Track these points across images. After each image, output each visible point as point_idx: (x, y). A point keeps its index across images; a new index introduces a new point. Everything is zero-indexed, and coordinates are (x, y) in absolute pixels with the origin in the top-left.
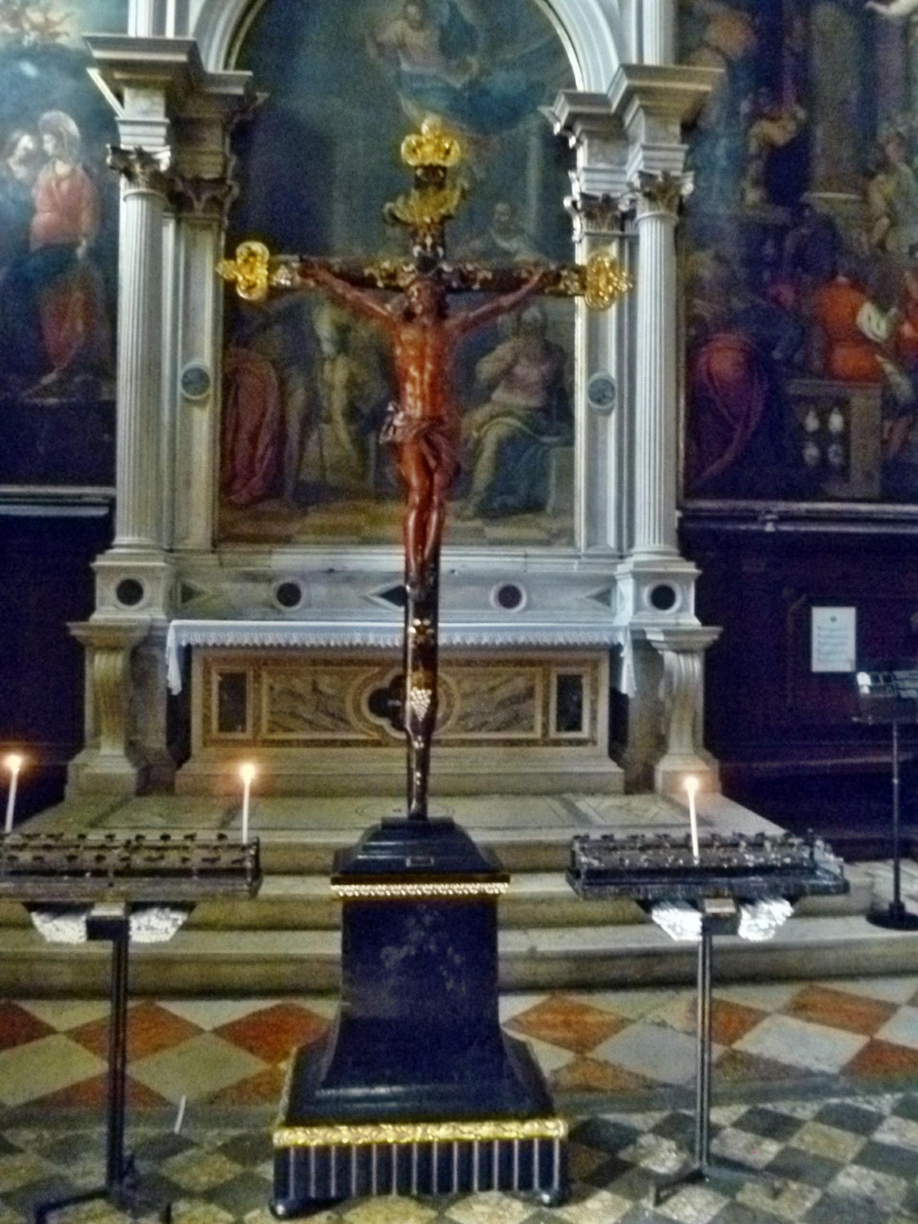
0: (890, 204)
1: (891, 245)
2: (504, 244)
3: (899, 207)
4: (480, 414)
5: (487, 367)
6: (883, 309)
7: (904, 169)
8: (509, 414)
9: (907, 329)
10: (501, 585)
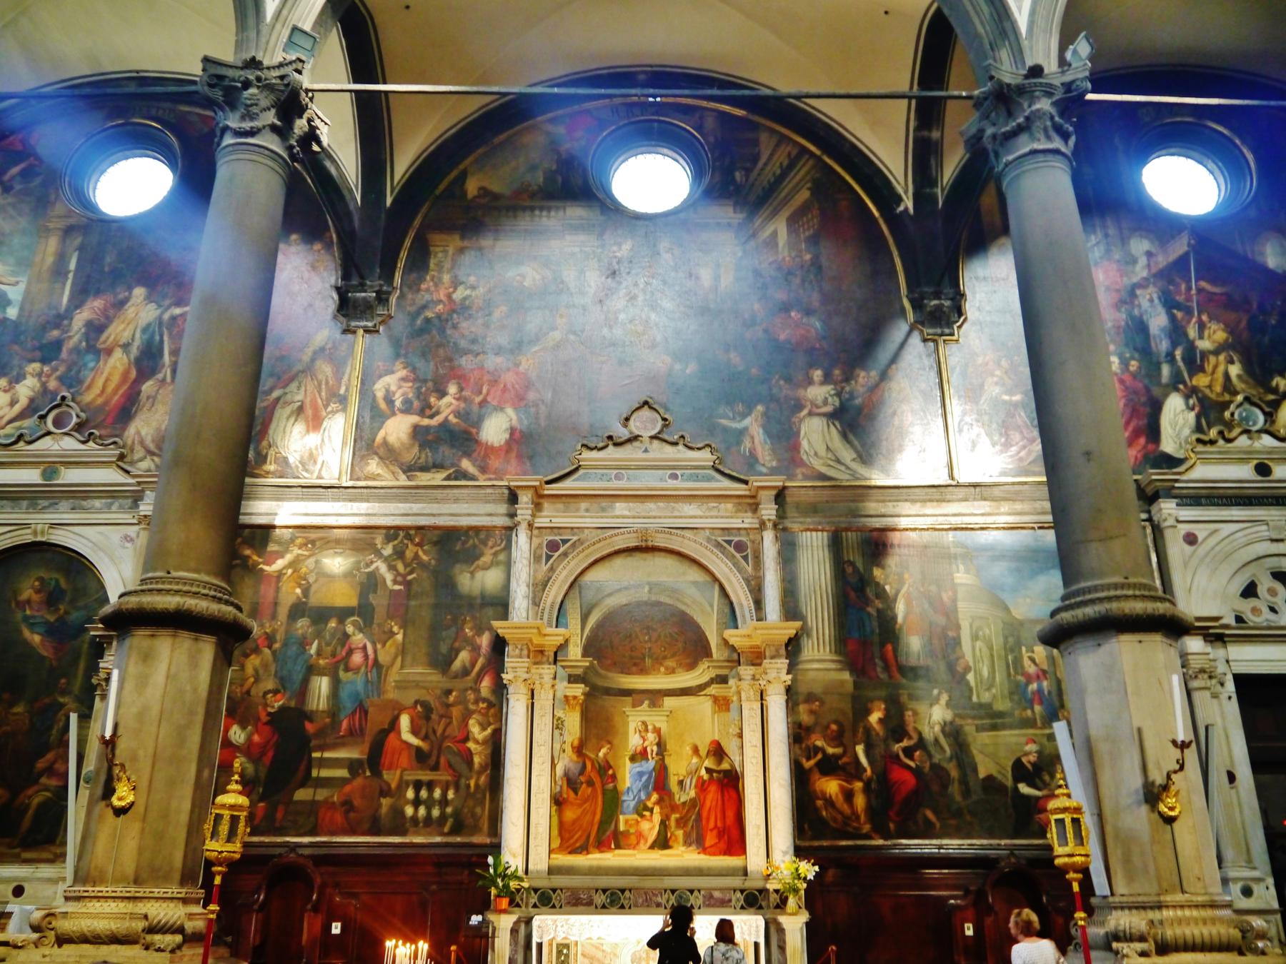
0: (256, 671)
1: (253, 692)
2: (61, 700)
3: (261, 672)
4: (30, 792)
5: (41, 764)
6: (243, 728)
7: (267, 651)
8: (47, 789)
9: (256, 738)
10: (15, 884)
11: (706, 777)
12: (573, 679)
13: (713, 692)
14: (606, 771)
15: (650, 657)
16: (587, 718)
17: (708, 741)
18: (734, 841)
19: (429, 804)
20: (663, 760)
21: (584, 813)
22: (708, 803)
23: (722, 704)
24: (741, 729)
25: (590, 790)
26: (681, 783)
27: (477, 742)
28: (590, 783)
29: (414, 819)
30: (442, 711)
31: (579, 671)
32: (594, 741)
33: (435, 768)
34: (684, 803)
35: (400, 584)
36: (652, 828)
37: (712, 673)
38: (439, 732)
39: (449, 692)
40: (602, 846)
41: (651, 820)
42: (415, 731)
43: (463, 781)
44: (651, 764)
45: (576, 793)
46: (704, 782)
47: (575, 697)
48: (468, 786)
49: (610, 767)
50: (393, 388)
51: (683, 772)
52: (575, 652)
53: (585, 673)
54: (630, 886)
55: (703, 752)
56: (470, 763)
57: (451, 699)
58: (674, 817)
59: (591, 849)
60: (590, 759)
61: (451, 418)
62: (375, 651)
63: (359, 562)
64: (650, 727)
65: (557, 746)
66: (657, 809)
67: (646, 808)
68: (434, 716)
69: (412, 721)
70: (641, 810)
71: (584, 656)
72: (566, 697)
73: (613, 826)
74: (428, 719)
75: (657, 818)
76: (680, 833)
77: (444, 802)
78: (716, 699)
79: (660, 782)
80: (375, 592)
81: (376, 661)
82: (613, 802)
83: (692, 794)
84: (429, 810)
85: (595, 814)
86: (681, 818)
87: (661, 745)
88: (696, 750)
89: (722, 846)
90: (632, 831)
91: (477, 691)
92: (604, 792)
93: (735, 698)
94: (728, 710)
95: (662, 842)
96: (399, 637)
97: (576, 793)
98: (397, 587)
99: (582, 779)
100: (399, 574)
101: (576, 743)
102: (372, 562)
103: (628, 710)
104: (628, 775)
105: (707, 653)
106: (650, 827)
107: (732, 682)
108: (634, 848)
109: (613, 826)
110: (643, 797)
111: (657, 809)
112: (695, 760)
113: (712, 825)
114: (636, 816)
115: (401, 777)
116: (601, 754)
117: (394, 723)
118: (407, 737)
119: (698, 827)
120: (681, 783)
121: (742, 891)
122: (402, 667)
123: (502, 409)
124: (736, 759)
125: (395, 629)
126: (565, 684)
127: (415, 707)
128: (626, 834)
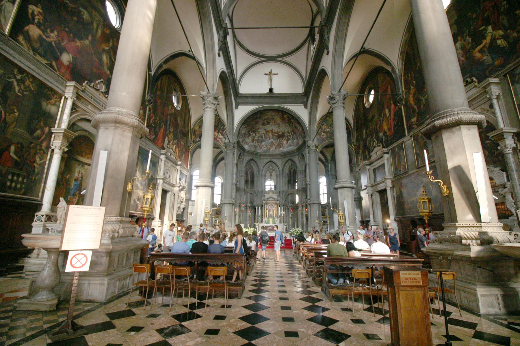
14: (68, 181)
19: (17, 182)
27: (37, 163)
29: (10, 187)
30: (28, 149)
33: (21, 169)
35: (21, 93)
38: (25, 157)
39: (32, 143)
42: (16, 153)
43: (30, 177)
44: (79, 183)
48: (32, 179)
50: (36, 13)
56: (34, 171)
57: (32, 146)
61: (53, 43)
62: (5, 115)
63: (4, 74)
68: (24, 150)
69: (15, 149)
74: (22, 150)
75: (77, 198)
77: (22, 183)
80: (10, 91)
81: (5, 119)
84: (16, 184)
87: (82, 178)
91: (41, 146)
92: (66, 188)
96: (17, 114)
98: (19, 94)
100: (21, 89)
102: (11, 78)
103: (76, 165)
115: (8, 169)
117: (8, 148)
118: (12, 154)
122: (15, 127)
123: (69, 53)
125: (16, 110)
127: (18, 144)
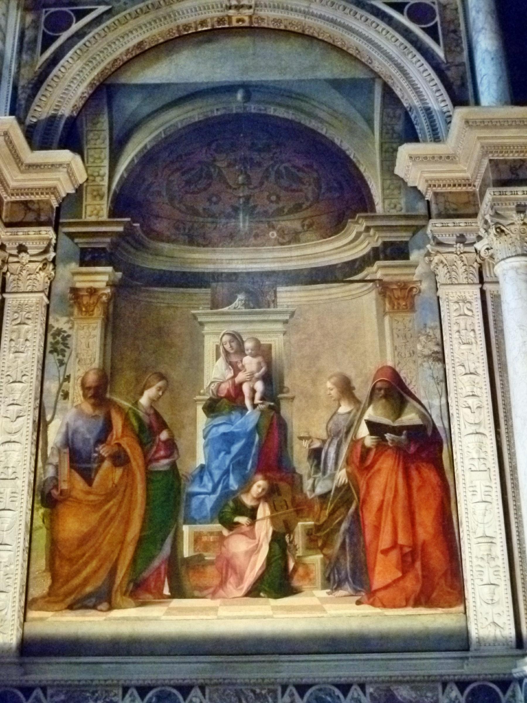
11: (369, 441)
12: (89, 257)
13: (378, 276)
15: (251, 212)
16: (112, 326)
17: (372, 366)
18: (438, 573)
20: (276, 409)
21: (107, 519)
22: (376, 497)
23: (399, 297)
24: (442, 345)
25: (119, 472)
26: (316, 455)
28: (120, 459)
31: (105, 242)
32: (129, 374)
34: (324, 497)
36: (256, 549)
37: (376, 240)
40: (140, 590)
41: (251, 535)
44: (252, 417)
45: (89, 481)
46: (369, 450)
47: (93, 292)
49: (163, 425)
51: (320, 431)
52: (96, 208)
53: (115, 245)
54: (201, 677)
55: (362, 391)
58: (302, 526)
59: (119, 599)
60: (120, 409)
64: (249, 345)
65: (52, 386)
66: (264, 511)
67: (240, 509)
70: (231, 512)
71: (112, 213)
72: (74, 291)
73: (167, 549)
75: (264, 529)
76: (315, 560)
78: (384, 288)
79: (270, 452)
82: (168, 498)
83: (342, 476)
85: (127, 522)
86: (318, 528)
87: (272, 380)
88: (346, 388)
89: (411, 584)
90: (209, 557)
92: (150, 477)
93: (424, 286)
94: (411, 308)
95: (277, 581)
97: (89, 481)
99: (104, 450)
101: (92, 379)
103: (202, 312)
104: (200, 442)
105: (363, 202)
106: (250, 549)
107: (415, 256)
108: (214, 595)
109: (167, 549)
110: (233, 484)
111: (264, 511)
112: (345, 408)
113: (385, 541)
114: (217, 526)
116: (144, 401)
119: (353, 545)
120: (316, 455)
121: (462, 685)
124: (434, 404)
126: (74, 266)
128: (197, 563)
